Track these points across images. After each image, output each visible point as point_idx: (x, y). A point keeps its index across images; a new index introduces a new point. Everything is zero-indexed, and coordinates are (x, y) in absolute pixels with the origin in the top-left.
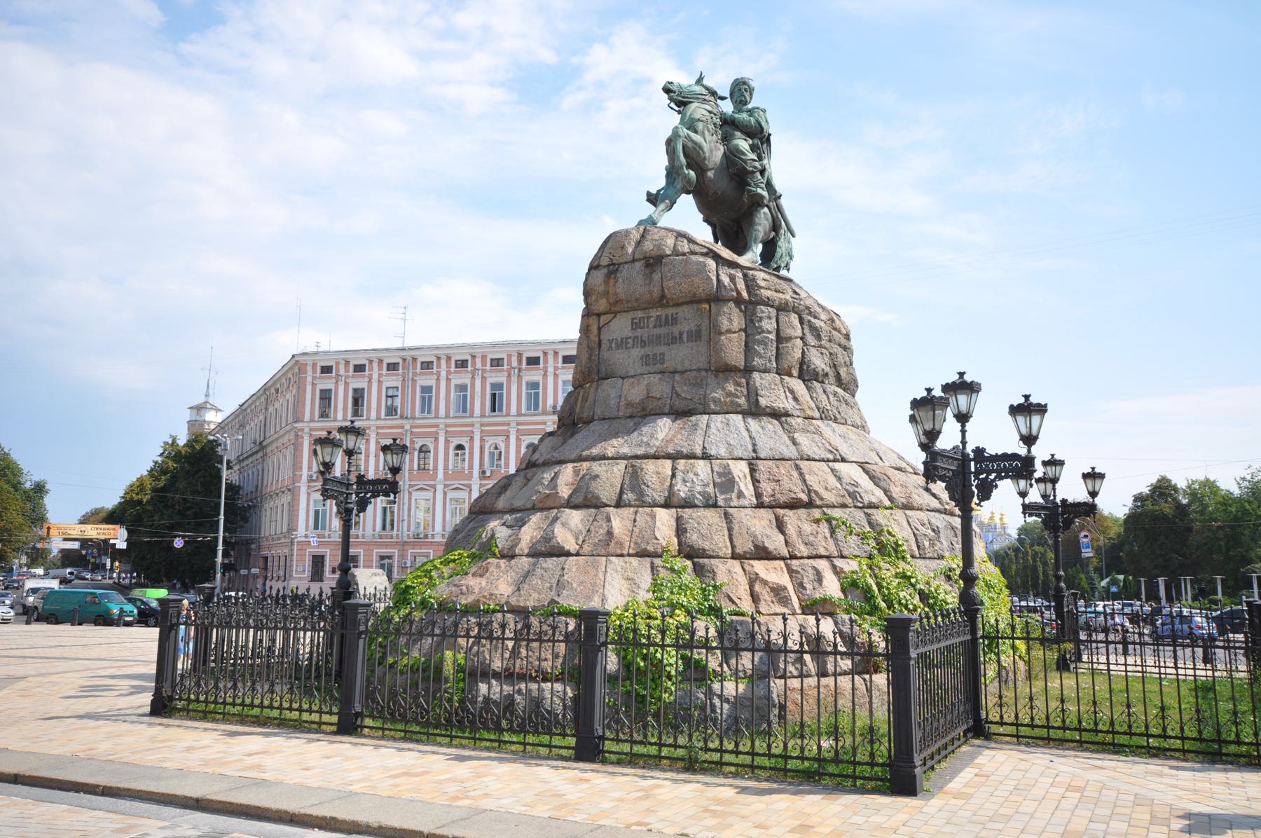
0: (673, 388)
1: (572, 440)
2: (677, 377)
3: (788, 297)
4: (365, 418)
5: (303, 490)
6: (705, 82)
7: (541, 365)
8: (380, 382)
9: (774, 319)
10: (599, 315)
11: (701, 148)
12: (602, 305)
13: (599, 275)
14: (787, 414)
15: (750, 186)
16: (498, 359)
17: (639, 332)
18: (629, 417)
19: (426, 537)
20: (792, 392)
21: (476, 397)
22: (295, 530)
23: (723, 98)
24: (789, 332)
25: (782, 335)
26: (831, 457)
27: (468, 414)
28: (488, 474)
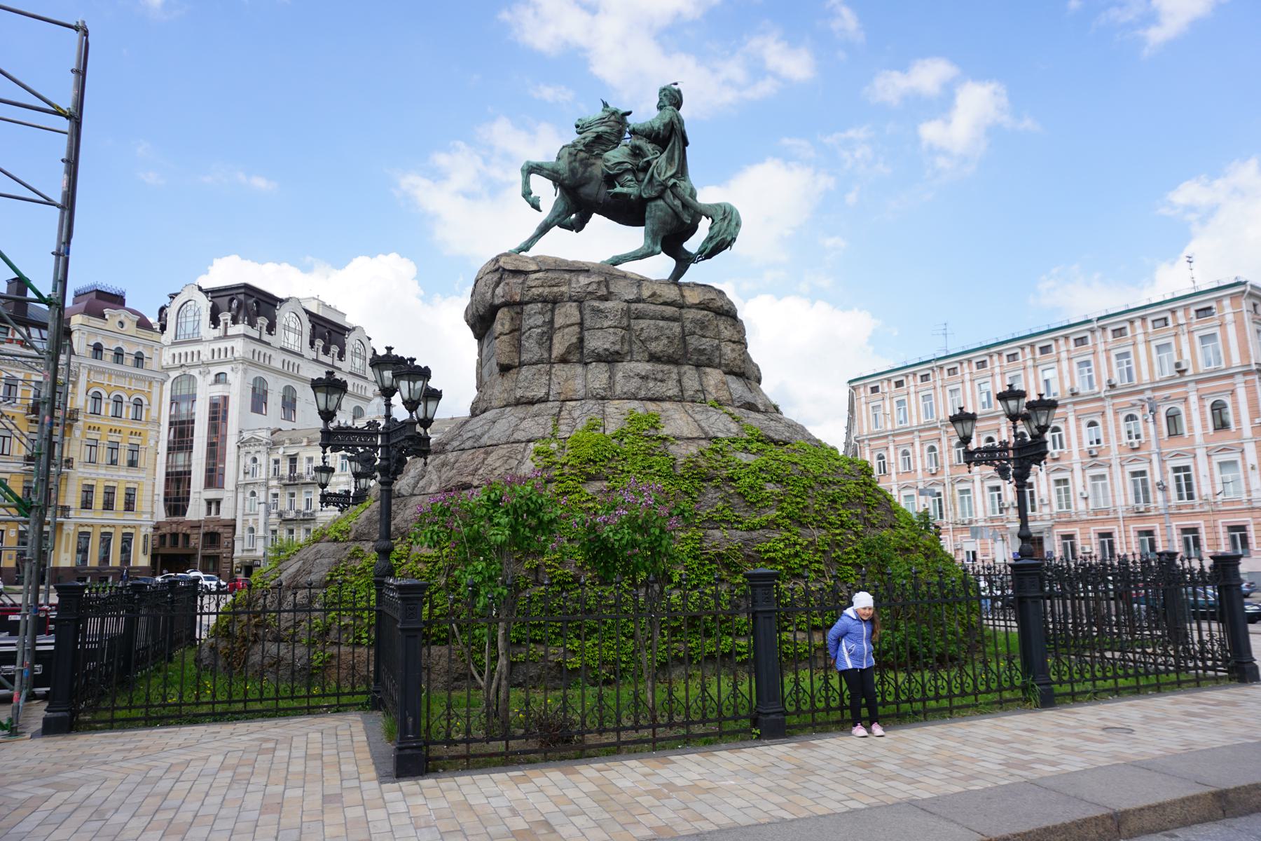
3: (564, 289)
6: (612, 106)
7: (1054, 352)
8: (916, 393)
9: (549, 313)
14: (540, 401)
19: (971, 522)
23: (629, 113)
24: (559, 321)
25: (557, 326)
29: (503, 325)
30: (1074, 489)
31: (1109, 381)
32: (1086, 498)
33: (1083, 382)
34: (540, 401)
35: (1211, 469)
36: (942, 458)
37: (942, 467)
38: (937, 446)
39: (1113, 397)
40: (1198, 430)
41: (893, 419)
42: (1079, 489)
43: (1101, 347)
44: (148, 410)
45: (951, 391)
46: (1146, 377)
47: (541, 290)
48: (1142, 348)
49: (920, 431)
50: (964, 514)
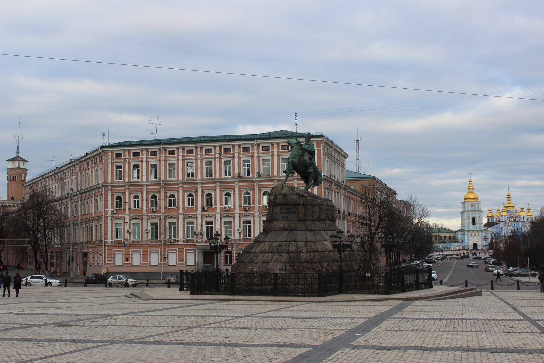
0: (290, 224)
1: (267, 236)
2: (291, 222)
3: (315, 202)
4: (140, 180)
5: (109, 219)
7: (232, 153)
8: (147, 162)
10: (272, 206)
11: (296, 163)
12: (273, 204)
13: (272, 197)
14: (315, 230)
15: (308, 170)
16: (209, 149)
17: (282, 211)
18: (281, 231)
19: (175, 241)
20: (316, 224)
21: (198, 169)
22: (106, 239)
24: (315, 211)
26: (323, 240)
27: (194, 178)
28: (206, 209)
29: (302, 210)
30: (234, 227)
31: (259, 173)
32: (240, 233)
34: (315, 230)
36: (160, 203)
37: (160, 208)
38: (158, 196)
39: (259, 181)
41: (129, 176)
42: (237, 227)
43: (256, 154)
45: (170, 164)
46: (276, 174)
47: (311, 202)
48: (275, 158)
49: (147, 185)
50: (170, 237)
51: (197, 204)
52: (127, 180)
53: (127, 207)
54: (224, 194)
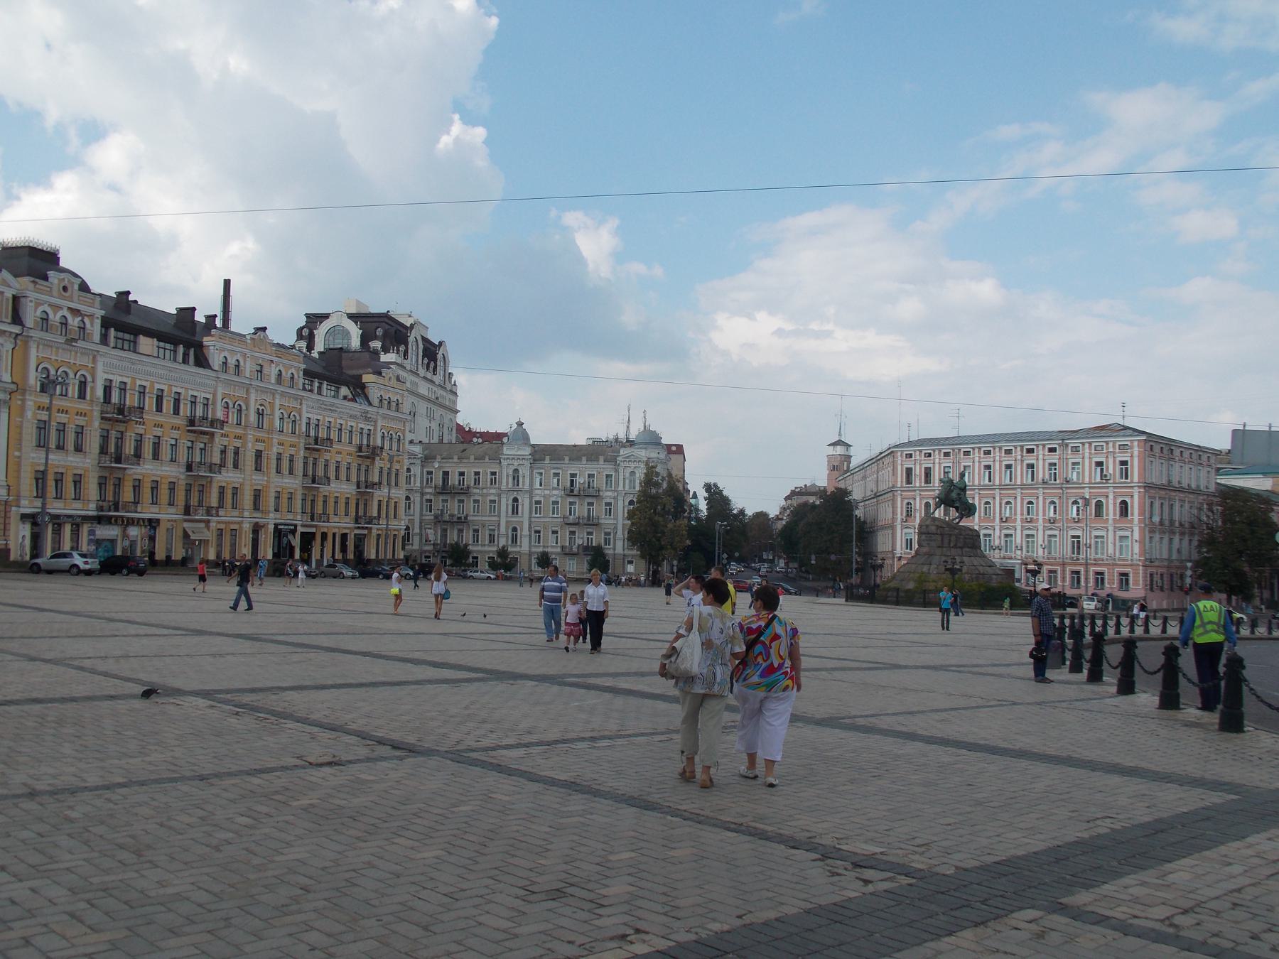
33: (1050, 477)
35: (1115, 539)
40: (1111, 516)
42: (1040, 542)
44: (403, 444)
46: (1087, 480)
51: (994, 513)
52: (918, 485)
53: (918, 515)
54: (1025, 502)
